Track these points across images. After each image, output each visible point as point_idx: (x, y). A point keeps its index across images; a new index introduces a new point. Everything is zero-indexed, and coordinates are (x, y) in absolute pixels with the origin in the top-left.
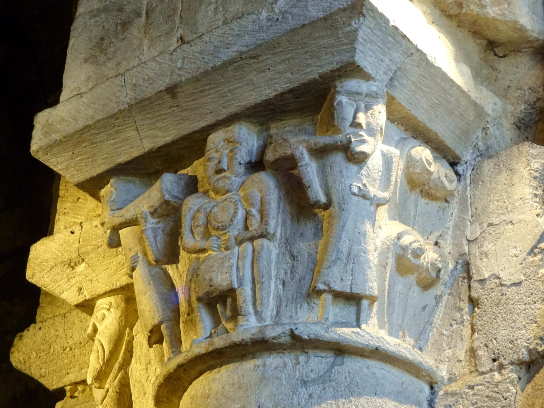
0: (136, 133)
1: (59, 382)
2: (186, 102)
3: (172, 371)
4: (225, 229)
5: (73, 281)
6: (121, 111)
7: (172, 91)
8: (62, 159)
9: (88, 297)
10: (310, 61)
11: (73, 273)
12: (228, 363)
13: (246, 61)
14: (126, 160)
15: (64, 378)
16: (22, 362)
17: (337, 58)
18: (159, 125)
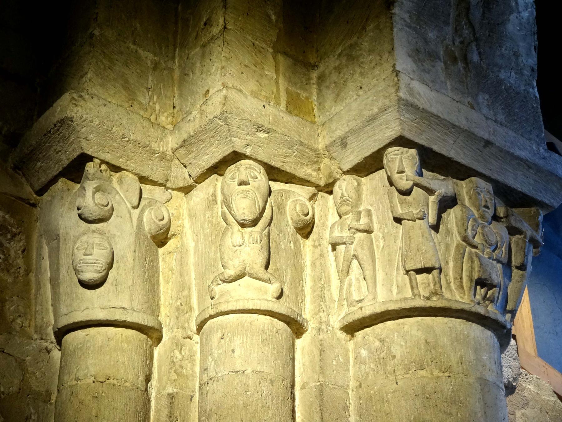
0: (453, 143)
1: (96, 152)
2: (486, 154)
3: (453, 307)
4: (490, 246)
6: (459, 127)
7: (488, 143)
8: (407, 116)
9: (248, 154)
10: (543, 191)
12: (477, 324)
13: (525, 165)
15: (103, 152)
16: (83, 119)
17: (552, 201)
18: (466, 151)
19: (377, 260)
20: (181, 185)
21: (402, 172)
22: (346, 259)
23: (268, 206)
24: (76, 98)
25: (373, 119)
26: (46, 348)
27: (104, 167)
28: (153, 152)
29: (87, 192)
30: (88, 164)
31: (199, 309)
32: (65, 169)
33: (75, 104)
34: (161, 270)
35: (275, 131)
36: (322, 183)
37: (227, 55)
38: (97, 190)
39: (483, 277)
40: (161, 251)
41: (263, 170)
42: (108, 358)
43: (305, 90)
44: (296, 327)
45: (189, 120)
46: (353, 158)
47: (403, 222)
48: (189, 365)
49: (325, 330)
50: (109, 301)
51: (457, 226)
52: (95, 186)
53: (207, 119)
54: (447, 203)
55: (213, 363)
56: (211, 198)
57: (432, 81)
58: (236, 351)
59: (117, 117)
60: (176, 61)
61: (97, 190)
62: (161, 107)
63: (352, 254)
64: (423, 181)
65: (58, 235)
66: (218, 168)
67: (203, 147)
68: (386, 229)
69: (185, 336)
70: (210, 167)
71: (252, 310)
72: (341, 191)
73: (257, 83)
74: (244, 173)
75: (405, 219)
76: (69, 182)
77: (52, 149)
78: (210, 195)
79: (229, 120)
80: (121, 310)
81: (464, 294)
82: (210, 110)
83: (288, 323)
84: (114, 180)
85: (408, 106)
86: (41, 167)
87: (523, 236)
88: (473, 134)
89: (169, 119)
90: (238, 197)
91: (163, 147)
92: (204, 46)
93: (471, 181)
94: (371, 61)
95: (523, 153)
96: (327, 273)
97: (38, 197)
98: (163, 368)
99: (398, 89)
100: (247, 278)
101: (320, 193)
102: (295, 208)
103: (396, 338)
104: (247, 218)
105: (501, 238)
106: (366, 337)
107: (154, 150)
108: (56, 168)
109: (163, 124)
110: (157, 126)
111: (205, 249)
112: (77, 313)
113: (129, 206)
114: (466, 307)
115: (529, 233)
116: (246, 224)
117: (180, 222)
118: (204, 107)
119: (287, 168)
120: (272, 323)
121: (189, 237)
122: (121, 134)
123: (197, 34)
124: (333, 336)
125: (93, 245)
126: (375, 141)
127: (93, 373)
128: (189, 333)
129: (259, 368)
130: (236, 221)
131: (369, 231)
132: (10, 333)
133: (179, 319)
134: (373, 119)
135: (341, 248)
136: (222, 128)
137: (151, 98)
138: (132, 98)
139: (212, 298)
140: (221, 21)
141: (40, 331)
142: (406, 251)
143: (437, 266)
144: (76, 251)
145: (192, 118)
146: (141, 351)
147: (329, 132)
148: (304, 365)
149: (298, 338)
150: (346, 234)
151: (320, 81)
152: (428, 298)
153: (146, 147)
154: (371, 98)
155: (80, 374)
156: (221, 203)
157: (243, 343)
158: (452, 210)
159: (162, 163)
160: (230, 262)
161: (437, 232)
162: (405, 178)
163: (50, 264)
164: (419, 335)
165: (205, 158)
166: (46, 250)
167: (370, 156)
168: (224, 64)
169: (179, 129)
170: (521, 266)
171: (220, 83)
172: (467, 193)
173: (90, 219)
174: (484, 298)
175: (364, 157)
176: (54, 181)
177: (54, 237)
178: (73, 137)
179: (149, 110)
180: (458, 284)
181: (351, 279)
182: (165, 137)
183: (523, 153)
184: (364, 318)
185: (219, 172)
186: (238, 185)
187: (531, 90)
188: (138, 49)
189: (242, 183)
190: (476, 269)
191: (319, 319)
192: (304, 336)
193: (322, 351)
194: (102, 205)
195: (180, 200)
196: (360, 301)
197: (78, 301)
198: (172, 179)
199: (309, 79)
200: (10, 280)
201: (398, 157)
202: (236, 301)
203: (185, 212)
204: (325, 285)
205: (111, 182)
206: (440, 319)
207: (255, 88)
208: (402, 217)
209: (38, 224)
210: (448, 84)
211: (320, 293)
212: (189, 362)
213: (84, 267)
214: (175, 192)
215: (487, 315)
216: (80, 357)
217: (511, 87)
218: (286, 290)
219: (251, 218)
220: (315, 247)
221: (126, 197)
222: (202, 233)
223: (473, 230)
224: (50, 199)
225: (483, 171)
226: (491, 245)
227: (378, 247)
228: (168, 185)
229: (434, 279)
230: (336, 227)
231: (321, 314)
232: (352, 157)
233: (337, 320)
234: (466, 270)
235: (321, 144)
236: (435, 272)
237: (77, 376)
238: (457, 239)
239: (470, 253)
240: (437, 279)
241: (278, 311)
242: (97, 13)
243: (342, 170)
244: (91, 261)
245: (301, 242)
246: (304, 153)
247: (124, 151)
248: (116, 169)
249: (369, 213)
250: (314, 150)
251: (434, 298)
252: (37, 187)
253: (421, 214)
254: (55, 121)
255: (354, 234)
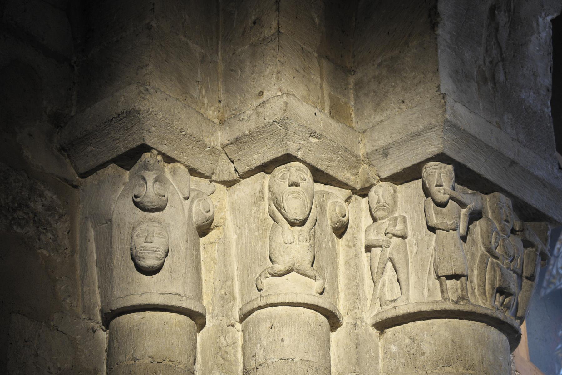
0: (483, 160)
5: (303, 142)
6: (491, 148)
7: (513, 163)
9: (299, 157)
11: (307, 139)
12: (495, 328)
14: (470, 168)
15: (162, 144)
16: (150, 112)
19: (410, 264)
20: (226, 178)
21: (441, 186)
22: (382, 261)
23: (313, 206)
24: (144, 91)
25: (417, 135)
26: (93, 328)
27: (159, 158)
28: (205, 147)
29: (148, 182)
30: (145, 154)
31: (242, 300)
32: (119, 156)
33: (143, 98)
34: (202, 258)
35: (325, 137)
36: (358, 187)
37: (282, 60)
38: (156, 180)
39: (503, 286)
40: (202, 240)
41: (309, 173)
42: (164, 340)
44: (334, 320)
45: (243, 119)
46: (392, 167)
47: (437, 231)
48: (232, 351)
49: (360, 326)
50: (165, 287)
51: (482, 237)
52: (154, 176)
53: (265, 122)
54: (475, 216)
55: (262, 350)
56: (258, 195)
57: (469, 102)
58: (285, 340)
59: (176, 112)
60: (220, 54)
61: (156, 180)
62: (208, 101)
63: (387, 257)
64: (459, 197)
65: (111, 220)
66: (267, 167)
67: (255, 147)
68: (420, 236)
69: (230, 324)
70: (259, 166)
71: (300, 303)
72: (377, 197)
73: (306, 88)
74: (295, 175)
75: (440, 229)
76: (120, 168)
77: (109, 136)
78: (257, 191)
79: (288, 125)
80: (177, 296)
81: (487, 301)
82: (268, 114)
83: (328, 318)
84: (166, 170)
85: (451, 127)
86: (92, 151)
87: (534, 249)
88: (502, 154)
89: (216, 113)
90: (289, 197)
91: (213, 141)
92: (254, 45)
93: (494, 196)
94: (414, 78)
95: (541, 173)
96: (361, 273)
97: (81, 179)
98: (208, 353)
99: (445, 111)
100: (294, 273)
101: (354, 196)
102: (335, 210)
103: (425, 336)
104: (299, 218)
105: (518, 250)
106: (397, 334)
107: (206, 145)
108: (109, 155)
109: (210, 117)
110: (208, 121)
111: (251, 243)
112: (135, 296)
113: (181, 197)
114: (489, 312)
115: (540, 247)
116: (296, 224)
117: (223, 214)
118: (260, 109)
119: (330, 172)
120: (316, 317)
121: (230, 228)
122: (180, 128)
123: (244, 31)
124: (366, 332)
125: (153, 233)
126: (417, 155)
127: (151, 354)
128: (233, 321)
129: (306, 358)
130: (286, 219)
131: (404, 237)
132: (62, 312)
133: (224, 308)
134: (417, 135)
135: (376, 251)
136: (280, 131)
137: (200, 91)
138: (185, 92)
139: (260, 290)
140: (274, 24)
141: (88, 310)
142: (440, 259)
143: (466, 274)
144: (135, 238)
145: (245, 117)
146: (191, 336)
147: (370, 140)
148: (339, 357)
149: (332, 331)
150: (382, 238)
151: (358, 87)
152: (456, 302)
153: (200, 141)
154: (416, 115)
155: (138, 354)
156: (269, 200)
157: (291, 333)
158: (478, 222)
159: (211, 157)
160: (281, 257)
161: (465, 243)
162: (442, 191)
163: (96, 247)
164: (447, 335)
165: (256, 156)
166: (92, 233)
167: (409, 168)
168: (279, 69)
169: (230, 126)
170: (531, 276)
171: (276, 87)
172: (490, 207)
173: (149, 208)
175: (403, 168)
176: (104, 165)
177: (105, 223)
178: (136, 128)
179: (200, 104)
180: (482, 291)
181: (384, 280)
182: (215, 131)
183: (541, 173)
184: (397, 317)
185: (266, 171)
186: (289, 186)
187: (546, 110)
188: (188, 41)
189: (294, 184)
190: (498, 278)
191: (355, 315)
192: (339, 329)
193: (357, 345)
194: (161, 196)
195: (222, 193)
196: (394, 301)
197: (134, 285)
198: (217, 172)
199: (347, 84)
200: (59, 260)
201: (437, 171)
202: (286, 294)
203: (226, 203)
204: (360, 284)
205: (164, 172)
206: (464, 322)
207: (305, 93)
208: (437, 227)
209: (81, 206)
210: (481, 104)
211: (355, 291)
212: (233, 349)
213: (146, 254)
214: (218, 185)
215: (505, 321)
216: (137, 338)
217: (529, 106)
218: (326, 287)
219: (302, 218)
220: (349, 246)
221: (178, 188)
222: (247, 228)
223: (496, 242)
224: (97, 183)
225: (505, 187)
226: (510, 256)
227: (411, 252)
228: (213, 178)
229: (462, 285)
230: (372, 231)
231: (356, 311)
232: (391, 166)
233: (370, 316)
234: (489, 279)
235: (361, 151)
236: (463, 279)
237: (134, 356)
238: (481, 249)
239: (492, 263)
240: (464, 285)
241: (323, 306)
242: (154, 4)
243: (379, 177)
244: (153, 249)
245: (336, 241)
246: (346, 159)
247: (180, 144)
248: (169, 160)
249: (404, 219)
250: (356, 157)
251: (462, 303)
252: (82, 170)
253: (455, 225)
254: (119, 111)
255: (391, 238)
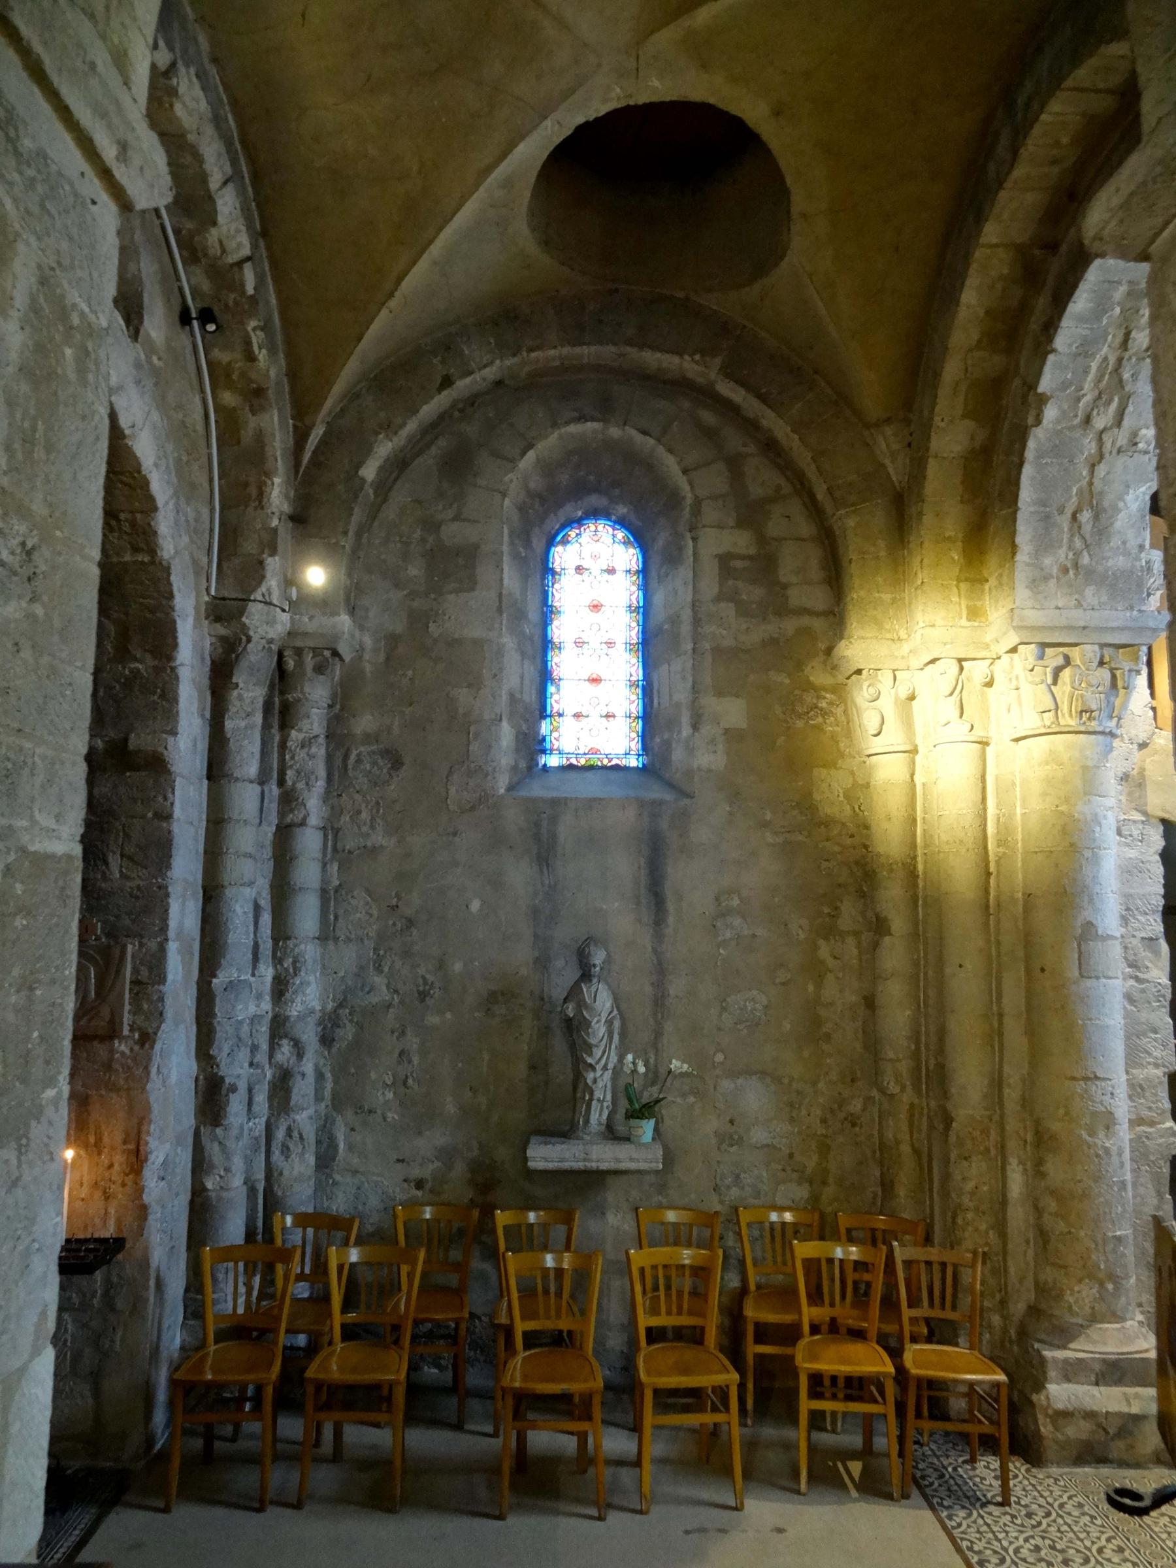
7: (1084, 628)
43: (980, 599)
174: (1089, 719)
249: (1017, 678)
